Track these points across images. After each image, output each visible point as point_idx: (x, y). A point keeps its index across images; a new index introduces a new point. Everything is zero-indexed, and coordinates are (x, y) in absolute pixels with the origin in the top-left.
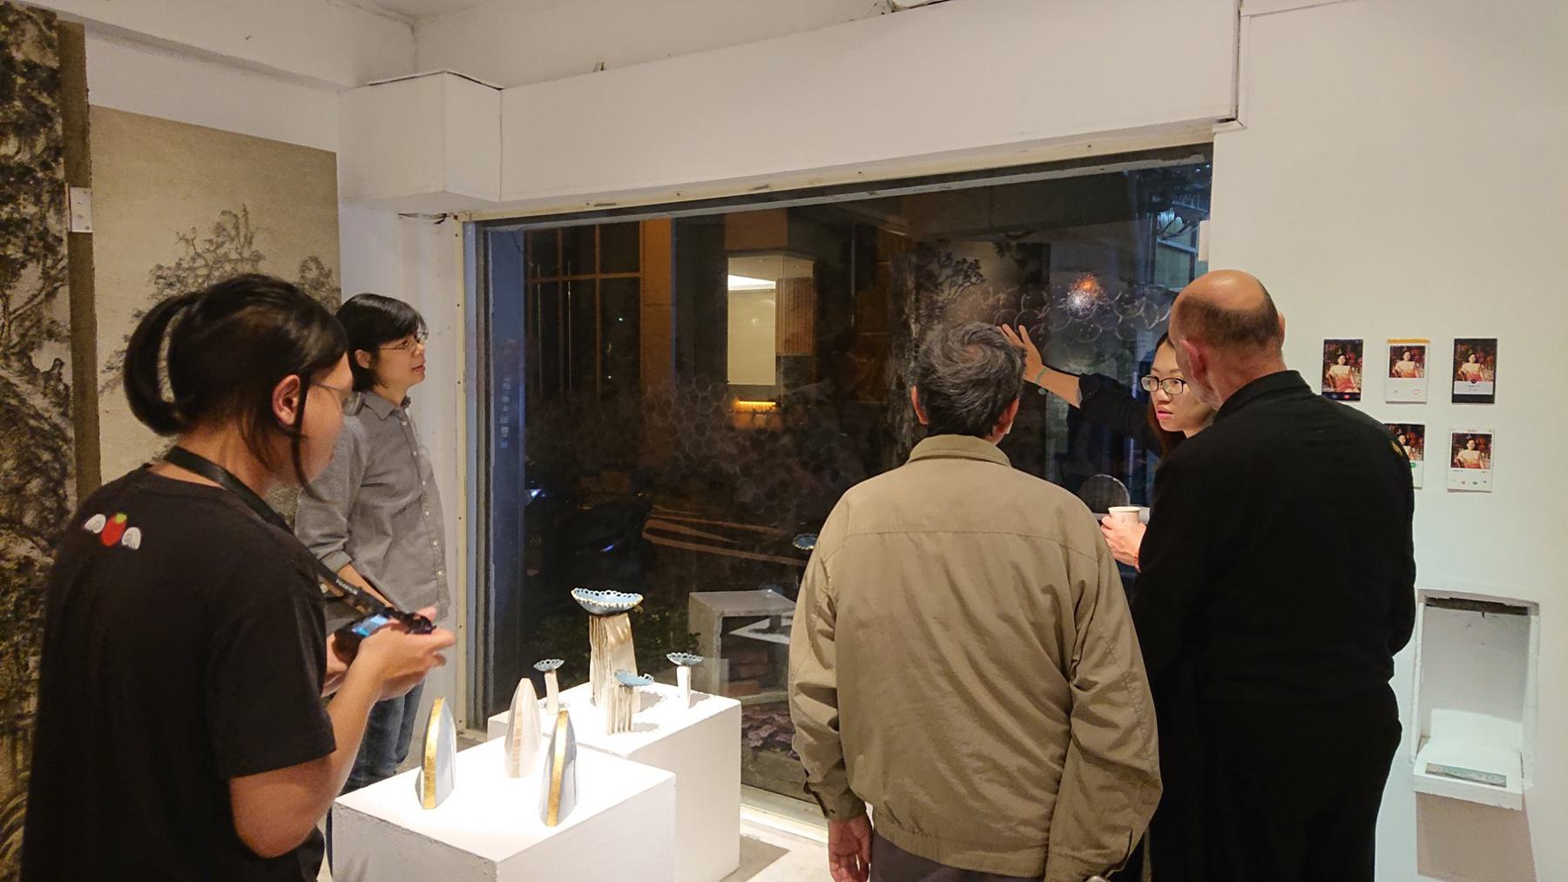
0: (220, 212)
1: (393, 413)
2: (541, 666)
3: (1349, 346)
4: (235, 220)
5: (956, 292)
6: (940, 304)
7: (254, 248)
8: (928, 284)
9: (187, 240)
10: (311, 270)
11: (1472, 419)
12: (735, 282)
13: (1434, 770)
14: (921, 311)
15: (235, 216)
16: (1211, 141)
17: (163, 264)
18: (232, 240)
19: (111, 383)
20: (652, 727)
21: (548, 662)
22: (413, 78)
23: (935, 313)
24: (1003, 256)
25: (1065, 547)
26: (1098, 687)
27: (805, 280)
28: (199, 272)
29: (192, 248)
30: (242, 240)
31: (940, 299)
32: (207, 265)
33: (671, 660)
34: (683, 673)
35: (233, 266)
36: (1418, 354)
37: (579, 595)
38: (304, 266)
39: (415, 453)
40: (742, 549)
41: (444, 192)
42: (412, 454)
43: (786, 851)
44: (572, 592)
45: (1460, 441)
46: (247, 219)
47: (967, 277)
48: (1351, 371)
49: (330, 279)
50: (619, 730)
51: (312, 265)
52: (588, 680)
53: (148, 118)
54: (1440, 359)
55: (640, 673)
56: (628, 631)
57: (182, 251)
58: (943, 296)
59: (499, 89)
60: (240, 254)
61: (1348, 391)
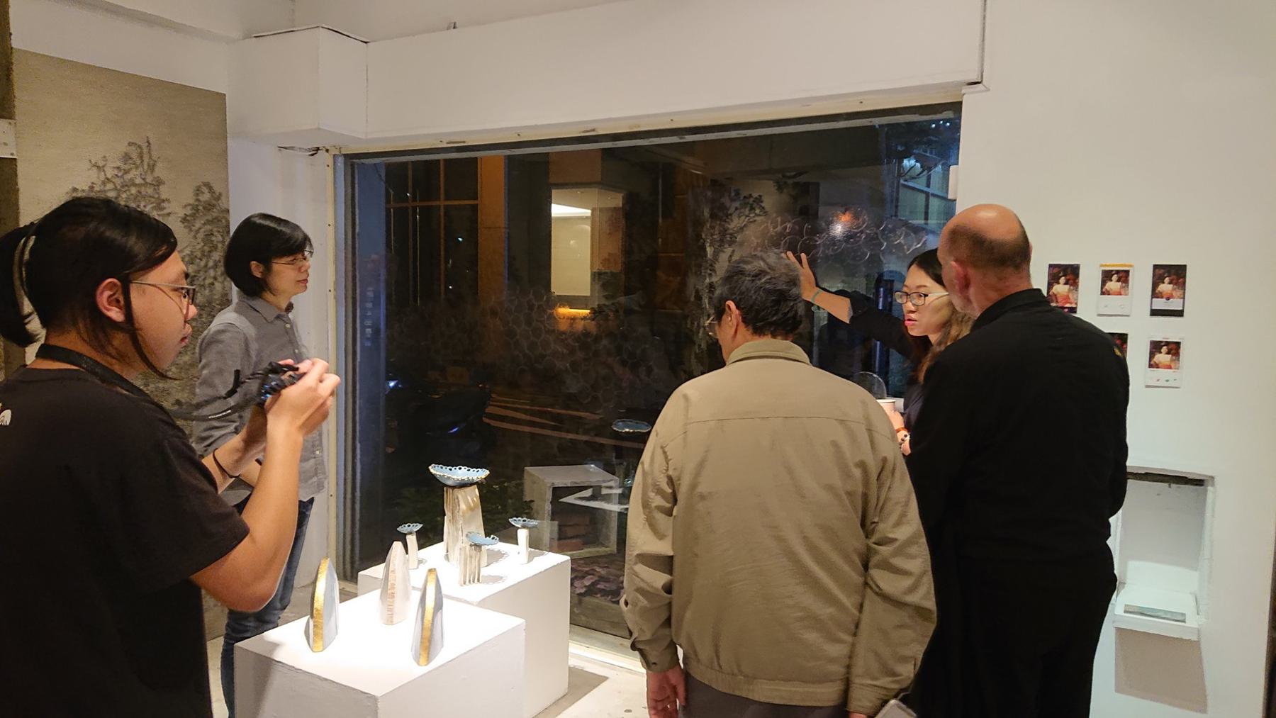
0: (127, 144)
1: (278, 317)
2: (403, 529)
5: (744, 221)
6: (731, 231)
7: (156, 174)
8: (721, 214)
10: (204, 193)
11: (1166, 329)
12: (558, 210)
13: (1130, 610)
14: (715, 237)
15: (140, 147)
16: (961, 100)
18: (137, 167)
20: (497, 579)
21: (409, 526)
23: (726, 238)
24: (782, 192)
25: (869, 430)
26: (897, 544)
27: (615, 209)
30: (146, 167)
31: (732, 226)
32: (115, 189)
33: (513, 523)
34: (523, 535)
35: (138, 189)
36: (1124, 276)
37: (435, 470)
38: (198, 190)
39: (297, 351)
40: (568, 431)
41: (319, 129)
42: (294, 352)
43: (606, 678)
44: (430, 467)
45: (1156, 347)
47: (752, 209)
48: (1070, 290)
49: (220, 202)
50: (470, 581)
51: (205, 190)
52: (442, 540)
53: (63, 61)
54: (1141, 280)
55: (487, 535)
56: (477, 500)
58: (735, 223)
59: (366, 43)
60: (144, 179)
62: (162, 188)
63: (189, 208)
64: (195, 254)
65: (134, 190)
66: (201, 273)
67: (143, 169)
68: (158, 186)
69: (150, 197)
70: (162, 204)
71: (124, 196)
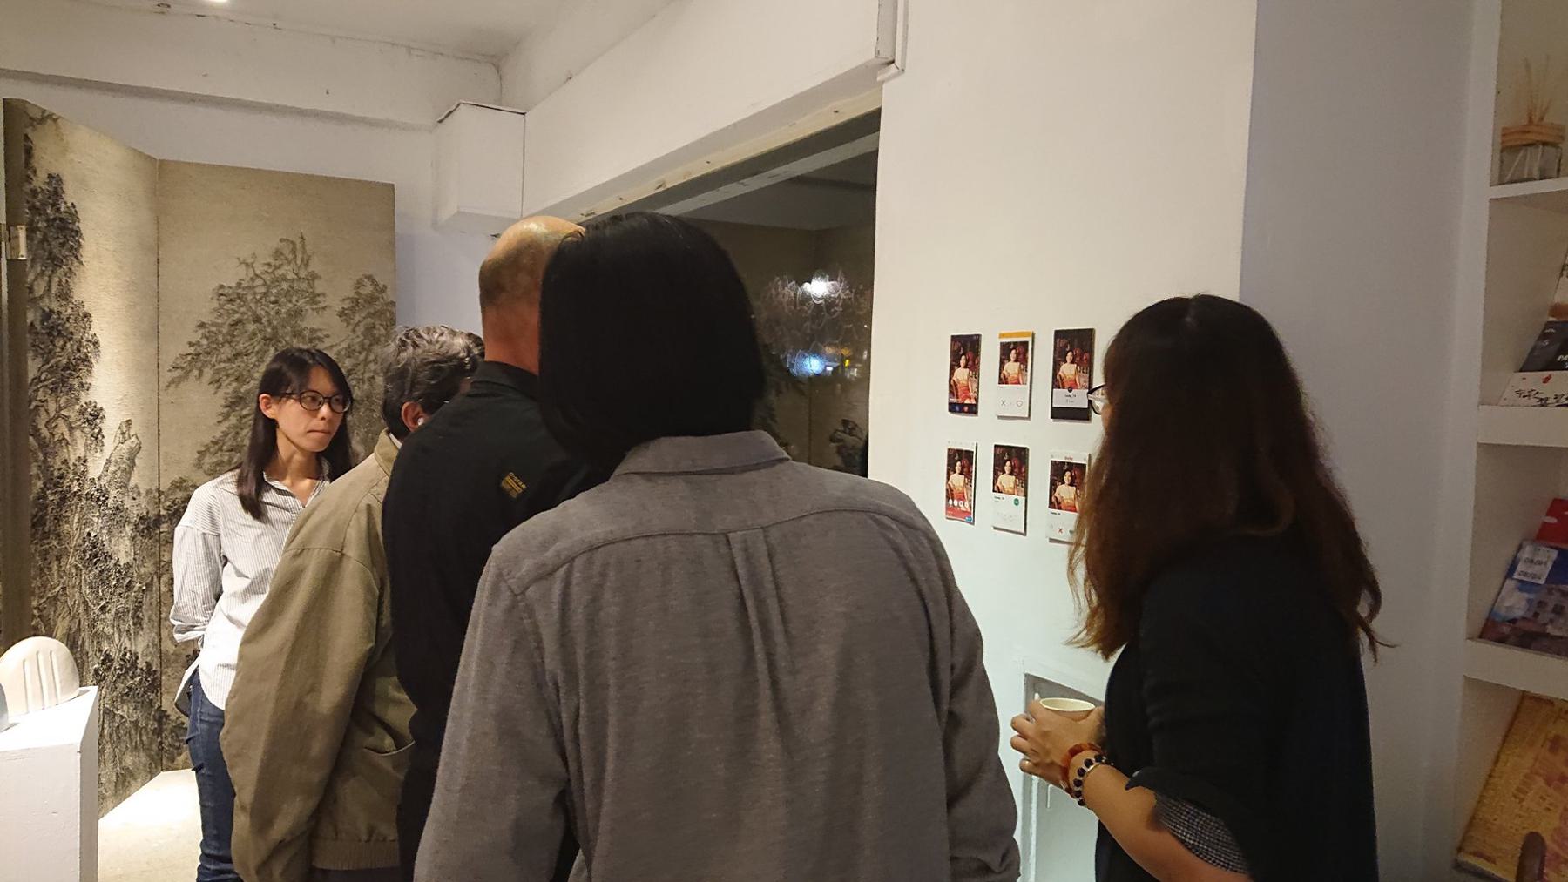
3: (969, 345)
4: (291, 246)
7: (310, 269)
9: (247, 265)
15: (293, 243)
17: (225, 284)
18: (289, 263)
19: (176, 380)
22: (451, 112)
28: (257, 290)
29: (251, 270)
30: (299, 262)
46: (303, 247)
49: (384, 294)
57: (242, 273)
60: (297, 274)
61: (967, 401)
62: (317, 282)
63: (348, 301)
64: (353, 348)
65: (285, 286)
66: (360, 367)
67: (296, 264)
68: (313, 279)
69: (303, 291)
70: (319, 299)
71: (274, 291)
